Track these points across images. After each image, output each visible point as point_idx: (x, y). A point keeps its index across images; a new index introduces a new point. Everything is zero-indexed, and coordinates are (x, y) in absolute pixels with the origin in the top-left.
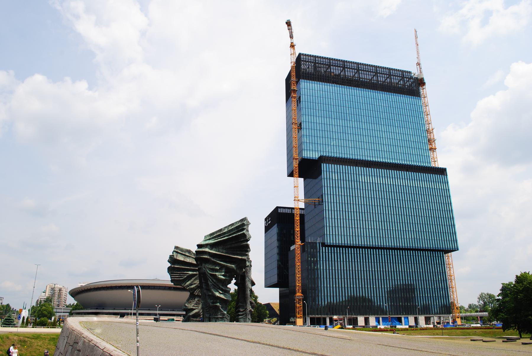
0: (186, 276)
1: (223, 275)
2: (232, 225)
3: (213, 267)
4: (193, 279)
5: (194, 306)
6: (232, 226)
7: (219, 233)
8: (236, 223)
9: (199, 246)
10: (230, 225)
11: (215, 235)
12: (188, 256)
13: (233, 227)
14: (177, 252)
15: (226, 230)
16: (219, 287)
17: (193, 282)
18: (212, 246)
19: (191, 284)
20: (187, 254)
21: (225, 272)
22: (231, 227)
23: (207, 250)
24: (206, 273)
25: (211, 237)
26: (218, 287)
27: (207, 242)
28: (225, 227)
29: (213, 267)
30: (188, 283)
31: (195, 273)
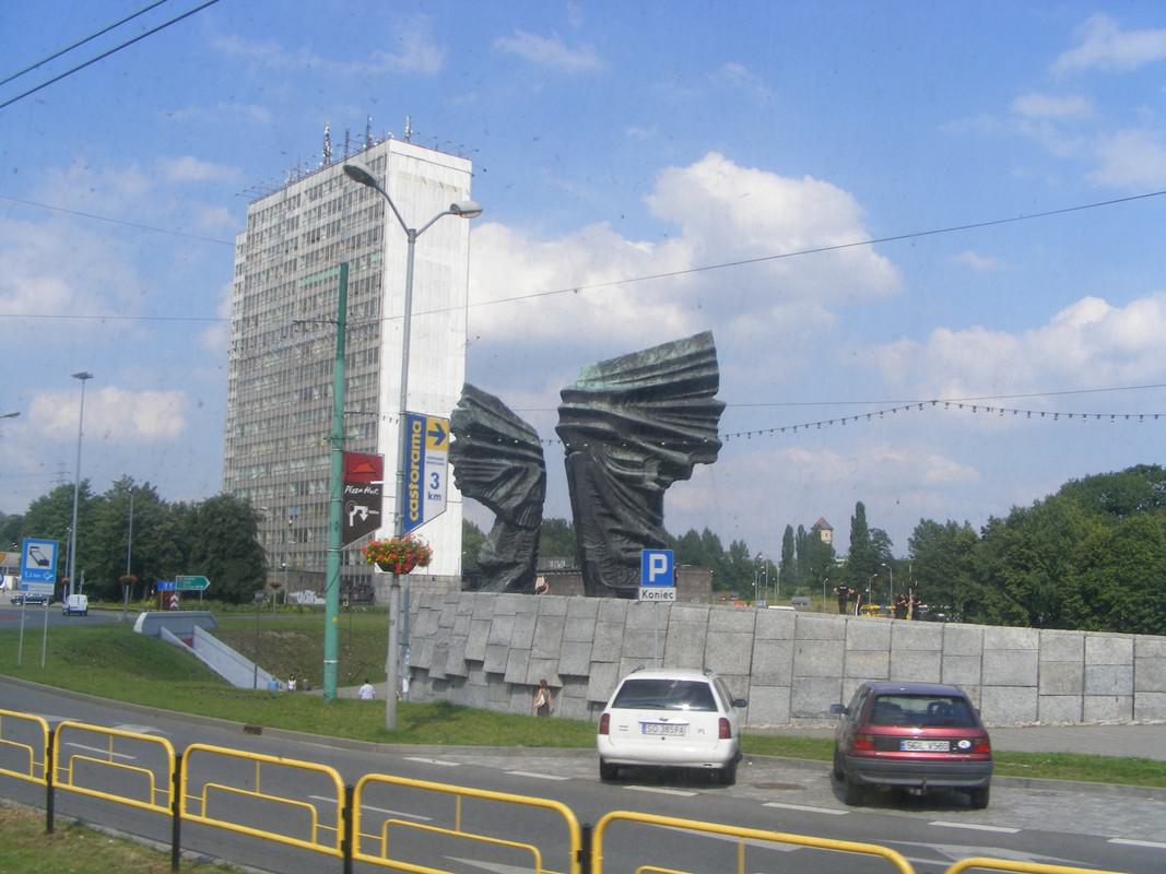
0: (499, 474)
1: (656, 481)
2: (670, 346)
3: (627, 457)
4: (514, 481)
5: (516, 556)
6: (669, 352)
7: (631, 366)
8: (683, 342)
9: (566, 395)
10: (662, 347)
11: (618, 371)
12: (496, 415)
13: (673, 355)
14: (473, 403)
15: (652, 361)
16: (644, 511)
17: (513, 489)
18: (616, 398)
19: (508, 496)
20: (492, 409)
21: (659, 473)
22: (665, 353)
23: (604, 407)
24: (605, 471)
25: (607, 373)
26: (639, 511)
27: (598, 386)
28: (649, 351)
29: (627, 457)
30: (502, 492)
31: (517, 464)
